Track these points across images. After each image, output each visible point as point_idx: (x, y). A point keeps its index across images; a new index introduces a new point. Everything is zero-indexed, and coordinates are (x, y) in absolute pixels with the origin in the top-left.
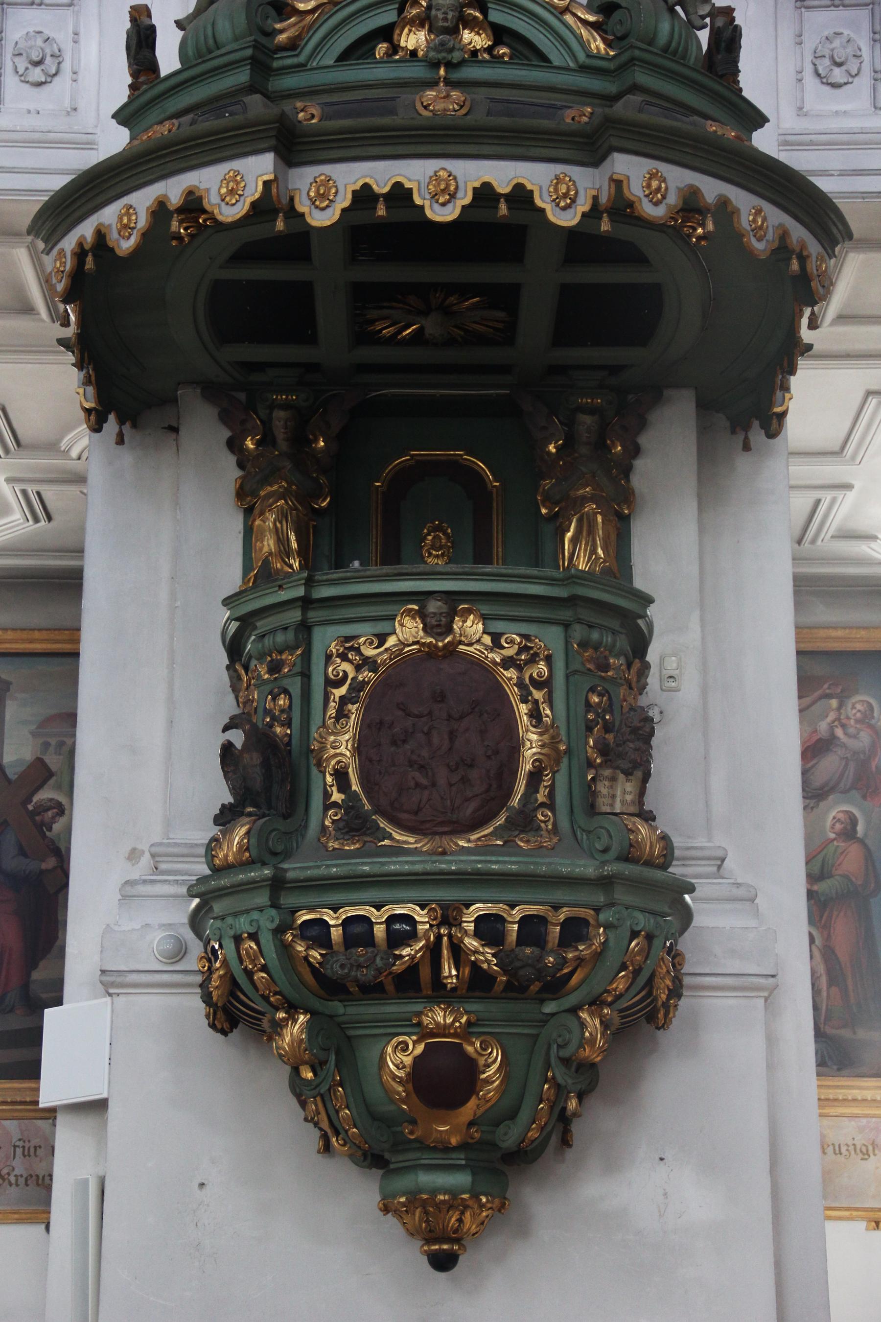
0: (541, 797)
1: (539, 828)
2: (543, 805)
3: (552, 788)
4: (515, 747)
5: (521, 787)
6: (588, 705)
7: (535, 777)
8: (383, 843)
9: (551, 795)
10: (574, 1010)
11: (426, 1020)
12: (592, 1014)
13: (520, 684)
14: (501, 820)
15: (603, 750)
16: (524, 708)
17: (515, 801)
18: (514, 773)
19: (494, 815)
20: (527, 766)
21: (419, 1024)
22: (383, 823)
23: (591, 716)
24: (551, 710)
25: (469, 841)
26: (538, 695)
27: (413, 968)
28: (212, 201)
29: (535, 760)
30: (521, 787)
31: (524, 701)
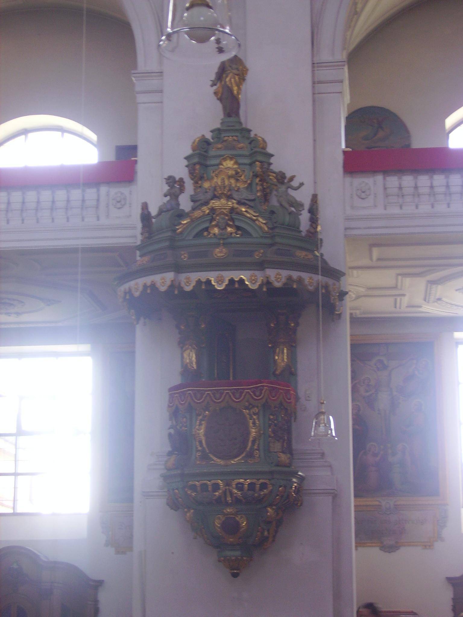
0: (256, 447)
1: (254, 457)
2: (256, 449)
3: (259, 444)
4: (249, 433)
5: (250, 444)
6: (270, 419)
7: (254, 442)
8: (212, 462)
9: (258, 447)
10: (266, 507)
11: (225, 511)
12: (270, 508)
13: (249, 414)
14: (243, 455)
15: (273, 432)
16: (251, 421)
17: (248, 449)
18: (248, 441)
19: (243, 453)
20: (251, 439)
21: (223, 512)
22: (212, 456)
23: (270, 422)
24: (259, 421)
25: (235, 461)
26: (255, 417)
27: (220, 497)
28: (158, 285)
29: (254, 437)
30: (250, 444)
31: (251, 420)
